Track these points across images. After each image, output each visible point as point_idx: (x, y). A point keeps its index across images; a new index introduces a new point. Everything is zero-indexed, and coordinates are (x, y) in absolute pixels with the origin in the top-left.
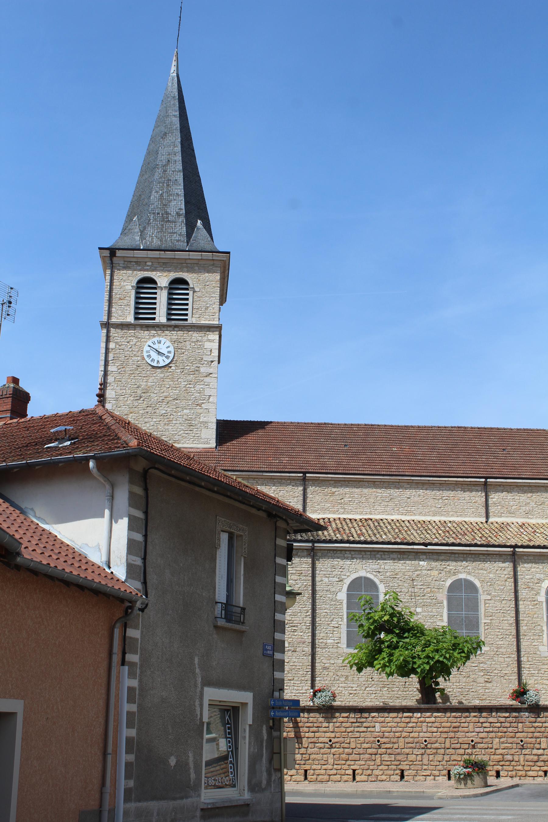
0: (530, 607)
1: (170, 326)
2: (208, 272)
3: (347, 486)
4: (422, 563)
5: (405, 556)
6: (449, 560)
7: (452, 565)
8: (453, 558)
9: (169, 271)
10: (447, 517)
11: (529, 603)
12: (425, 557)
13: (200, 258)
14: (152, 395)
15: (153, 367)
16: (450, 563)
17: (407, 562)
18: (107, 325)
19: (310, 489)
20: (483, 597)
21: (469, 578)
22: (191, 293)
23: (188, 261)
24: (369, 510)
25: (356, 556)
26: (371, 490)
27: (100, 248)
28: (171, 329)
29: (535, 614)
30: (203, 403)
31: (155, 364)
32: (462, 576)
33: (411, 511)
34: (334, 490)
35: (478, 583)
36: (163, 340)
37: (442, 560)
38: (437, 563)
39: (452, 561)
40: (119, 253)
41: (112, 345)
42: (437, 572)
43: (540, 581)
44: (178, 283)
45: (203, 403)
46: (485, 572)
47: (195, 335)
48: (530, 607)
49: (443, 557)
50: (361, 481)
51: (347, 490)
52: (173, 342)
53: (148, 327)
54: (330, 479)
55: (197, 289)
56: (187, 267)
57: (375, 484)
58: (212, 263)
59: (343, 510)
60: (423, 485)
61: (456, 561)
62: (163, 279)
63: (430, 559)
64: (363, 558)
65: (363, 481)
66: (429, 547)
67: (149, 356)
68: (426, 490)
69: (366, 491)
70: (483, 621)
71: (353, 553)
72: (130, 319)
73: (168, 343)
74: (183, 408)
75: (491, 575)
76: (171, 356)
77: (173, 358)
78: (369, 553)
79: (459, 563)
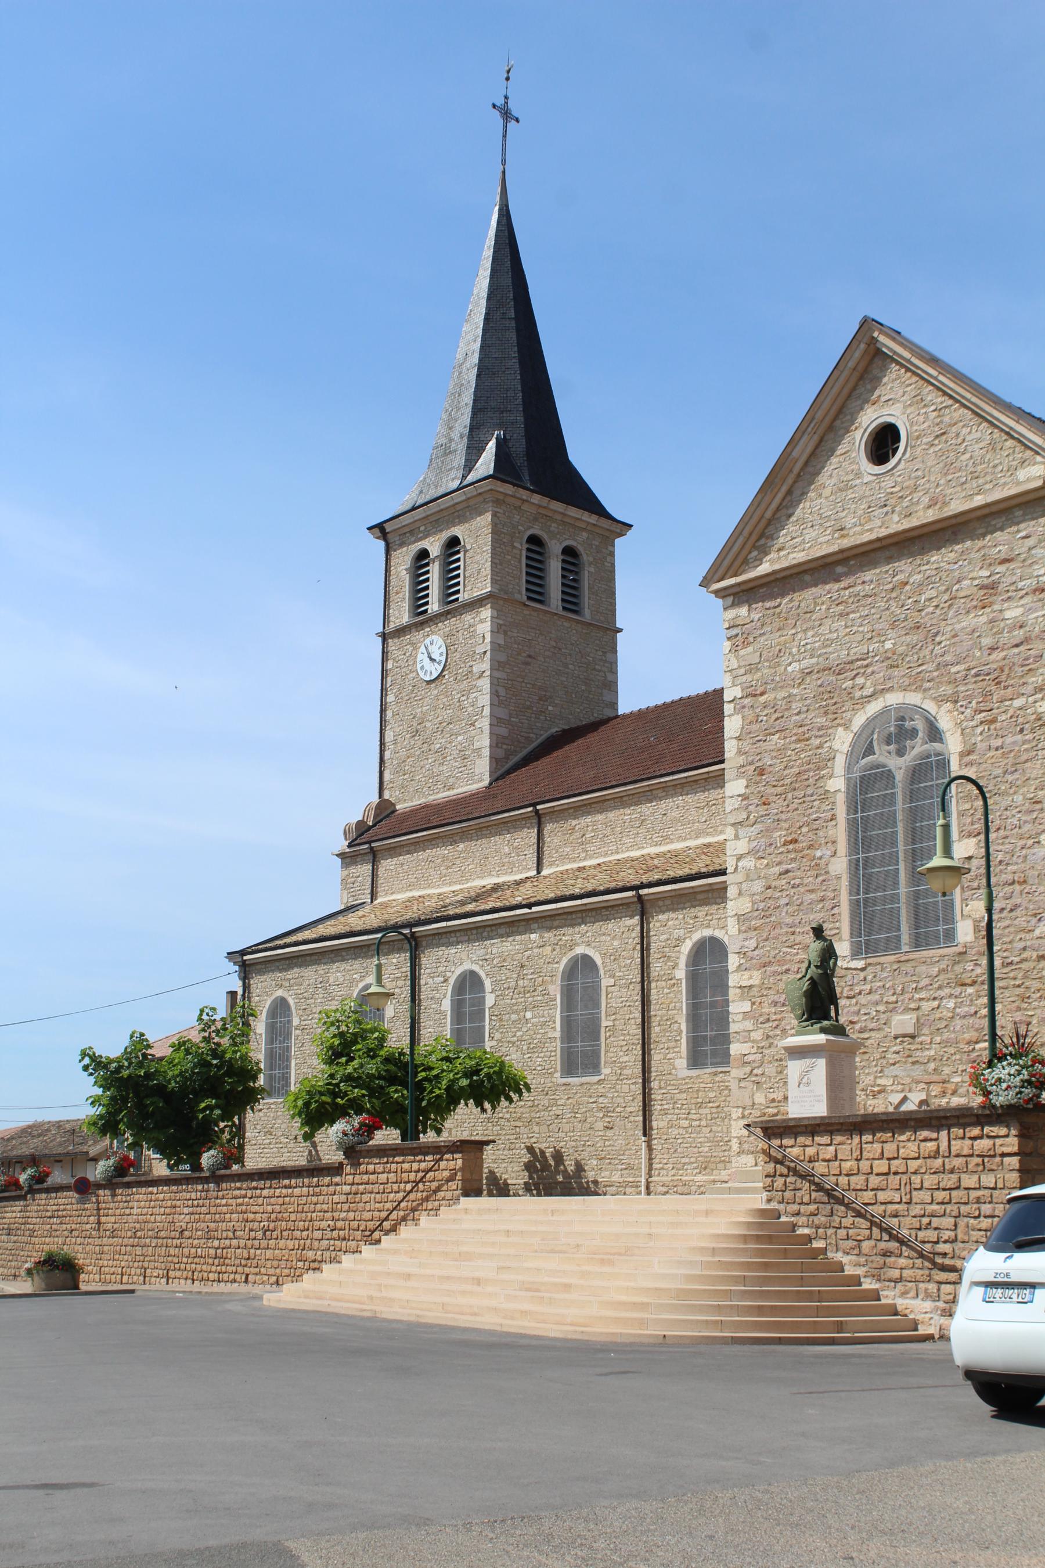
0: (666, 991)
1: (448, 612)
2: (480, 515)
3: (589, 813)
4: (533, 936)
5: (515, 929)
6: (565, 926)
7: (568, 934)
8: (568, 922)
9: (441, 531)
10: (713, 836)
11: (664, 983)
12: (536, 925)
13: (464, 498)
14: (428, 724)
15: (429, 682)
16: (565, 930)
17: (517, 938)
18: (384, 637)
19: (548, 828)
20: (606, 982)
21: (587, 952)
22: (461, 555)
23: (458, 507)
24: (614, 848)
25: (462, 938)
26: (617, 812)
27: (369, 529)
28: (443, 618)
29: (671, 1002)
30: (476, 720)
31: (428, 678)
32: (580, 950)
33: (667, 837)
34: (574, 822)
35: (598, 960)
36: (435, 637)
37: (557, 928)
38: (550, 934)
39: (568, 926)
40: (388, 527)
41: (390, 665)
42: (550, 948)
43: (680, 941)
44: (453, 542)
45: (476, 720)
46: (609, 938)
47: (468, 618)
48: (666, 991)
49: (556, 923)
50: (605, 801)
51: (589, 819)
52: (446, 637)
53: (421, 625)
54: (566, 807)
55: (468, 547)
56: (458, 517)
57: (622, 802)
58: (481, 498)
59: (584, 855)
60: (682, 788)
61: (572, 926)
62: (434, 546)
63: (543, 927)
64: (469, 941)
65: (605, 801)
66: (534, 909)
67: (422, 668)
68: (687, 794)
69: (611, 815)
70: (604, 1023)
71: (458, 934)
72: (405, 618)
73: (441, 642)
74: (458, 734)
75: (616, 943)
76: (443, 658)
77: (446, 661)
78: (474, 932)
79: (577, 929)
